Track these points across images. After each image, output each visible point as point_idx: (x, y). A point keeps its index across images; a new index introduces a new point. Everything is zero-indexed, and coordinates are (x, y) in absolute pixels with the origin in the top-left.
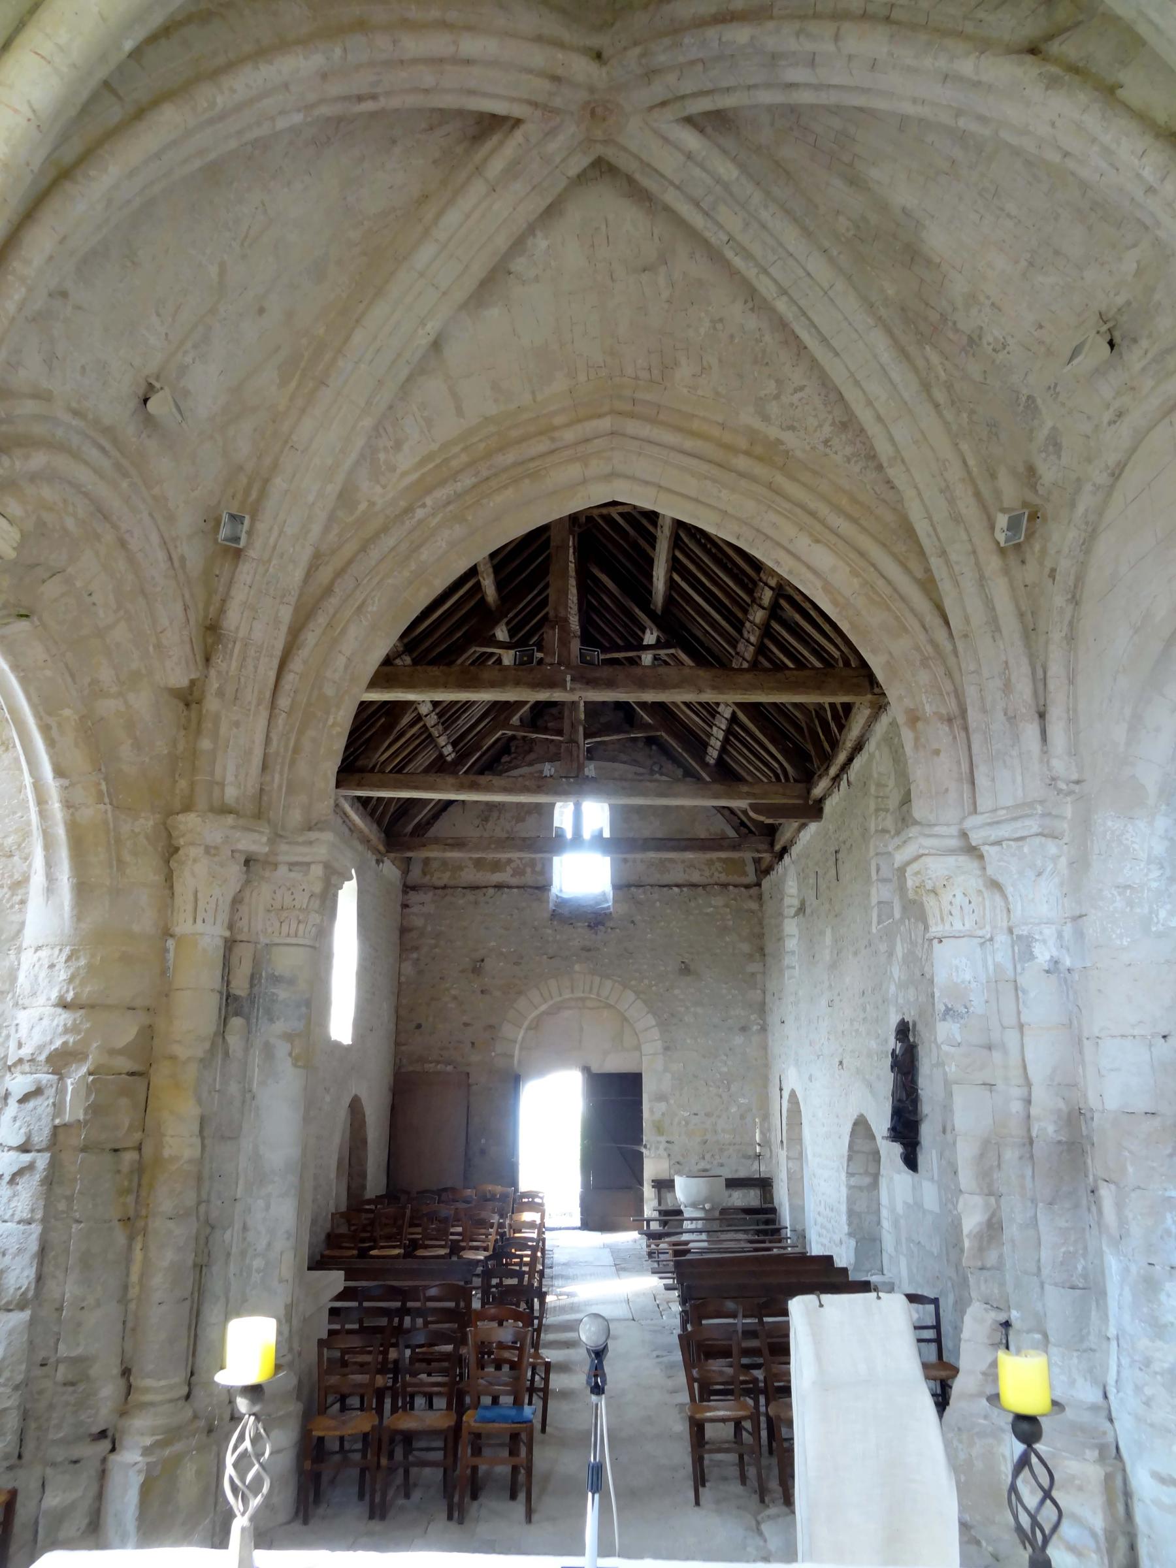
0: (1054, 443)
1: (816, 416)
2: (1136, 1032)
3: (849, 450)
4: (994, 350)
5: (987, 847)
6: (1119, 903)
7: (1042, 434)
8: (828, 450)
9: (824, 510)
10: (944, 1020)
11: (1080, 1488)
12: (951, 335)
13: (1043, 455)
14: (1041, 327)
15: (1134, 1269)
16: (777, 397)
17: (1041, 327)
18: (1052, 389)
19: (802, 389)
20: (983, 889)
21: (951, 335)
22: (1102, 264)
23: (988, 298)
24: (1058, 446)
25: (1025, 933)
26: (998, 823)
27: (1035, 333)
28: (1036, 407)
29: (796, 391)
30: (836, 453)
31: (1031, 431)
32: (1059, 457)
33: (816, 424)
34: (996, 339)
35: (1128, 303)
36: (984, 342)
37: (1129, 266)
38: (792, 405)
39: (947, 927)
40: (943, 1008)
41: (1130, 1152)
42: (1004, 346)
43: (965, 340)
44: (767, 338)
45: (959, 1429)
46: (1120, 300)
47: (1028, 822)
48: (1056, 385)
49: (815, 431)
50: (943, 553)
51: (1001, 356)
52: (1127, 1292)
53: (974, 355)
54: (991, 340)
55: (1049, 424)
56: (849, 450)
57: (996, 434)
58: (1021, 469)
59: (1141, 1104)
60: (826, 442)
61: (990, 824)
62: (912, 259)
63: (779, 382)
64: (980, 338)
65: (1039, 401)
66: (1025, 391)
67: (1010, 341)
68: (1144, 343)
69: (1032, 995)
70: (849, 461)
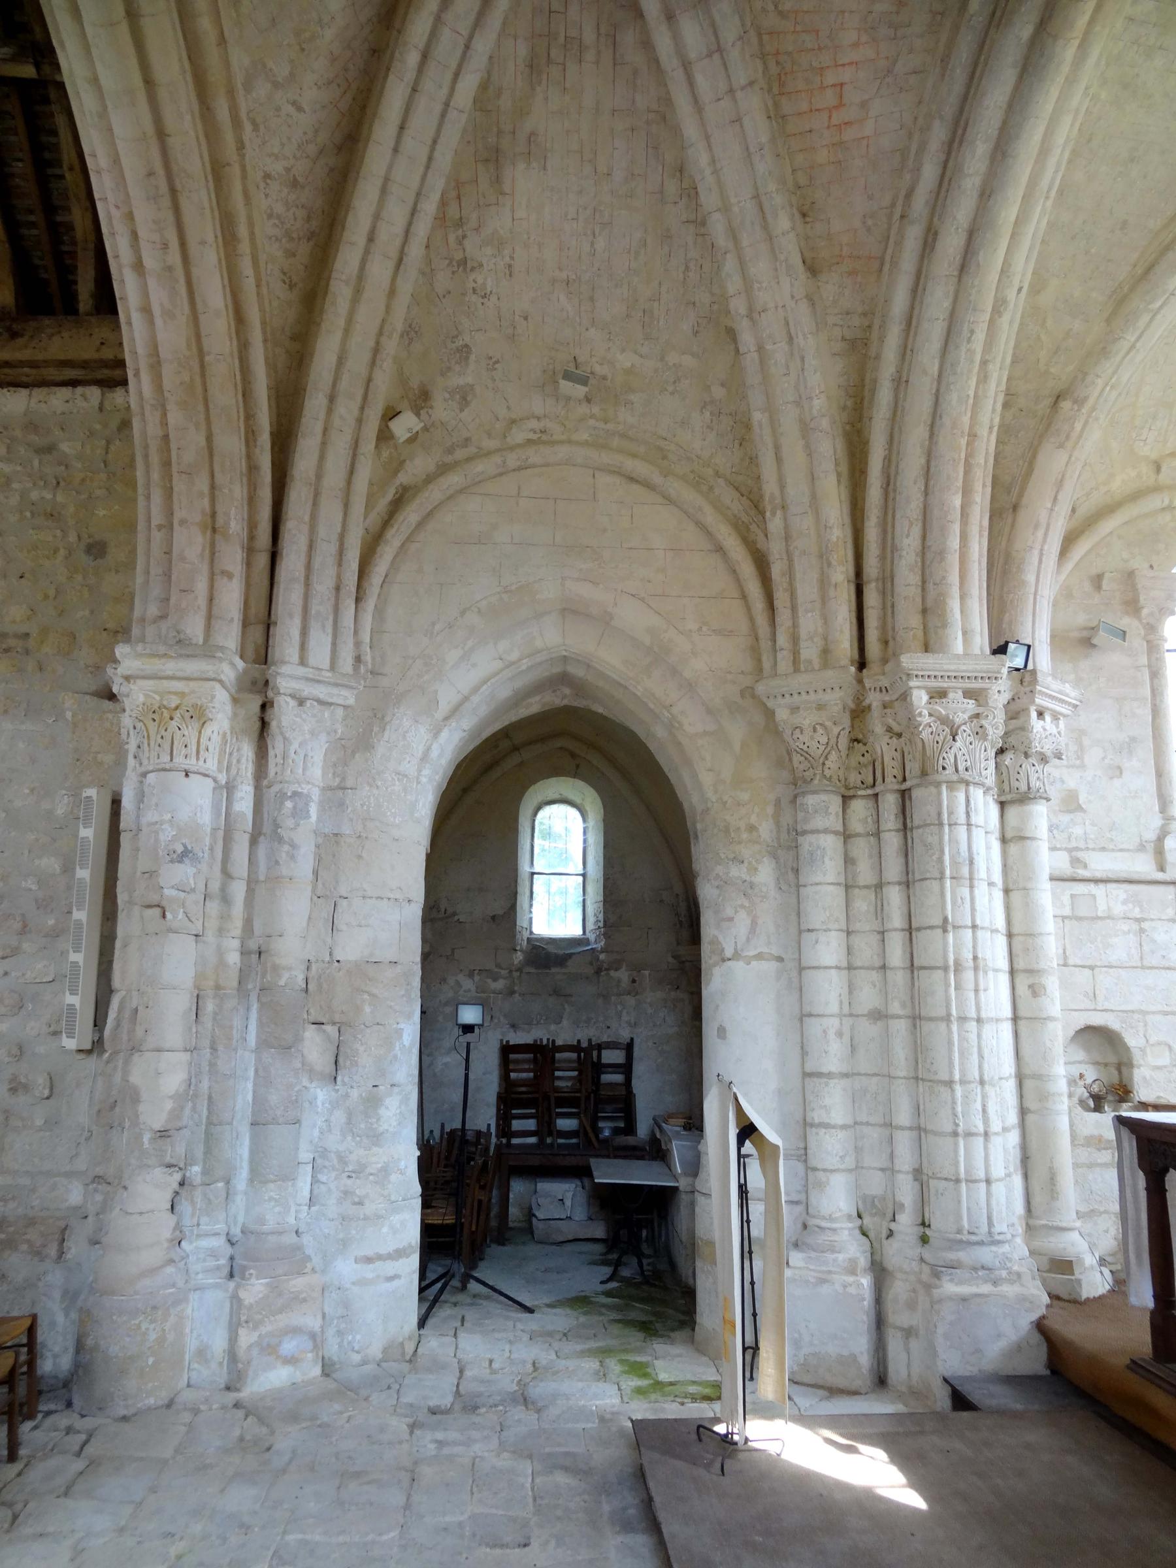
0: (464, 397)
1: (283, 145)
2: (392, 896)
3: (279, 208)
4: (474, 290)
5: (289, 699)
6: (397, 787)
7: (457, 381)
8: (262, 185)
9: (244, 247)
10: (181, 862)
11: (305, 1300)
12: (452, 238)
13: (447, 396)
14: (526, 318)
15: (355, 1093)
16: (276, 85)
17: (526, 318)
18: (493, 363)
19: (300, 109)
20: (229, 732)
21: (452, 238)
22: (609, 339)
23: (512, 258)
24: (464, 402)
25: (305, 791)
26: (318, 682)
27: (517, 317)
28: (467, 358)
29: (294, 103)
30: (267, 196)
31: (449, 369)
32: (462, 410)
33: (276, 151)
34: (484, 284)
35: (604, 378)
36: (473, 276)
37: (625, 360)
38: (278, 109)
39: (201, 762)
40: (180, 849)
41: (370, 994)
42: (484, 297)
43: (459, 256)
44: (329, 34)
45: (155, 1308)
46: (599, 370)
47: (345, 692)
48: (497, 362)
49: (270, 156)
50: (332, 399)
51: (474, 298)
52: (339, 1117)
53: (453, 273)
54: (480, 281)
55: (470, 380)
56: (279, 208)
57: (411, 340)
58: (415, 383)
59: (389, 955)
60: (267, 176)
61: (308, 679)
62: (487, 160)
63: (292, 74)
64: (473, 269)
65: (473, 357)
66: (467, 339)
67: (494, 299)
68: (596, 410)
69: (302, 851)
70: (270, 216)
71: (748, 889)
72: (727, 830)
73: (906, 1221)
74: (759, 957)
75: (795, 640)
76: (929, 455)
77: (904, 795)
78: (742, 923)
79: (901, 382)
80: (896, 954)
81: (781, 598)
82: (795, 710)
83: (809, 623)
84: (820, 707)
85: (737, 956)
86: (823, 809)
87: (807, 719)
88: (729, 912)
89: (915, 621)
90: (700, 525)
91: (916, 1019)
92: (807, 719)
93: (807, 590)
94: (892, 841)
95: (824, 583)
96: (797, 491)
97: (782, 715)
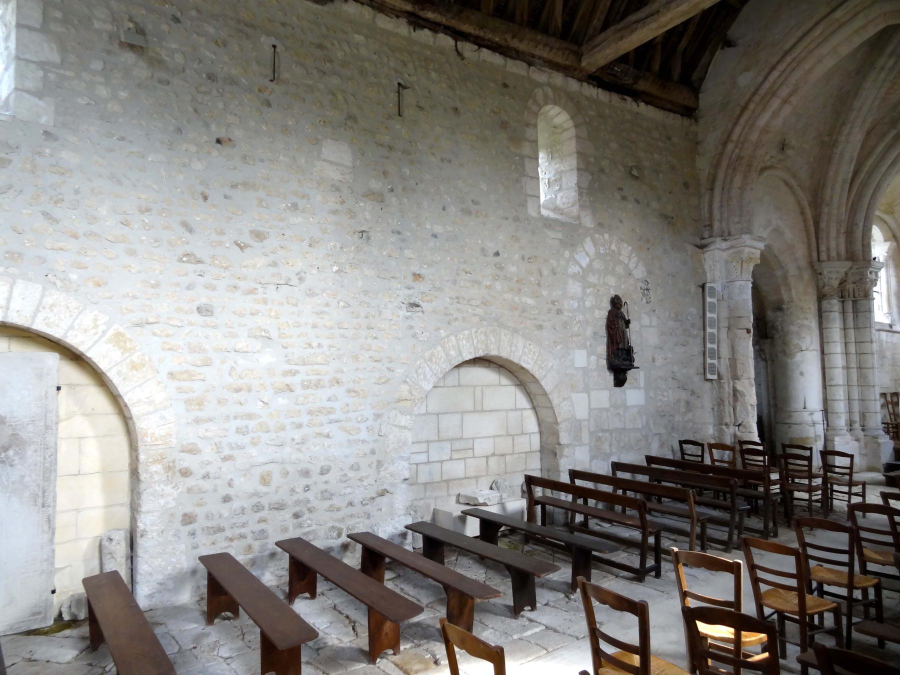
71: (809, 328)
72: (802, 308)
73: (857, 426)
74: (813, 350)
75: (828, 249)
76: (871, 198)
77: (855, 302)
78: (808, 340)
79: (870, 174)
80: (852, 349)
81: (823, 235)
82: (830, 272)
83: (833, 244)
84: (838, 272)
85: (807, 350)
86: (834, 305)
87: (834, 276)
88: (804, 335)
89: (861, 248)
90: (799, 204)
91: (860, 368)
92: (834, 276)
93: (833, 233)
94: (850, 316)
95: (838, 232)
96: (836, 199)
97: (825, 272)
